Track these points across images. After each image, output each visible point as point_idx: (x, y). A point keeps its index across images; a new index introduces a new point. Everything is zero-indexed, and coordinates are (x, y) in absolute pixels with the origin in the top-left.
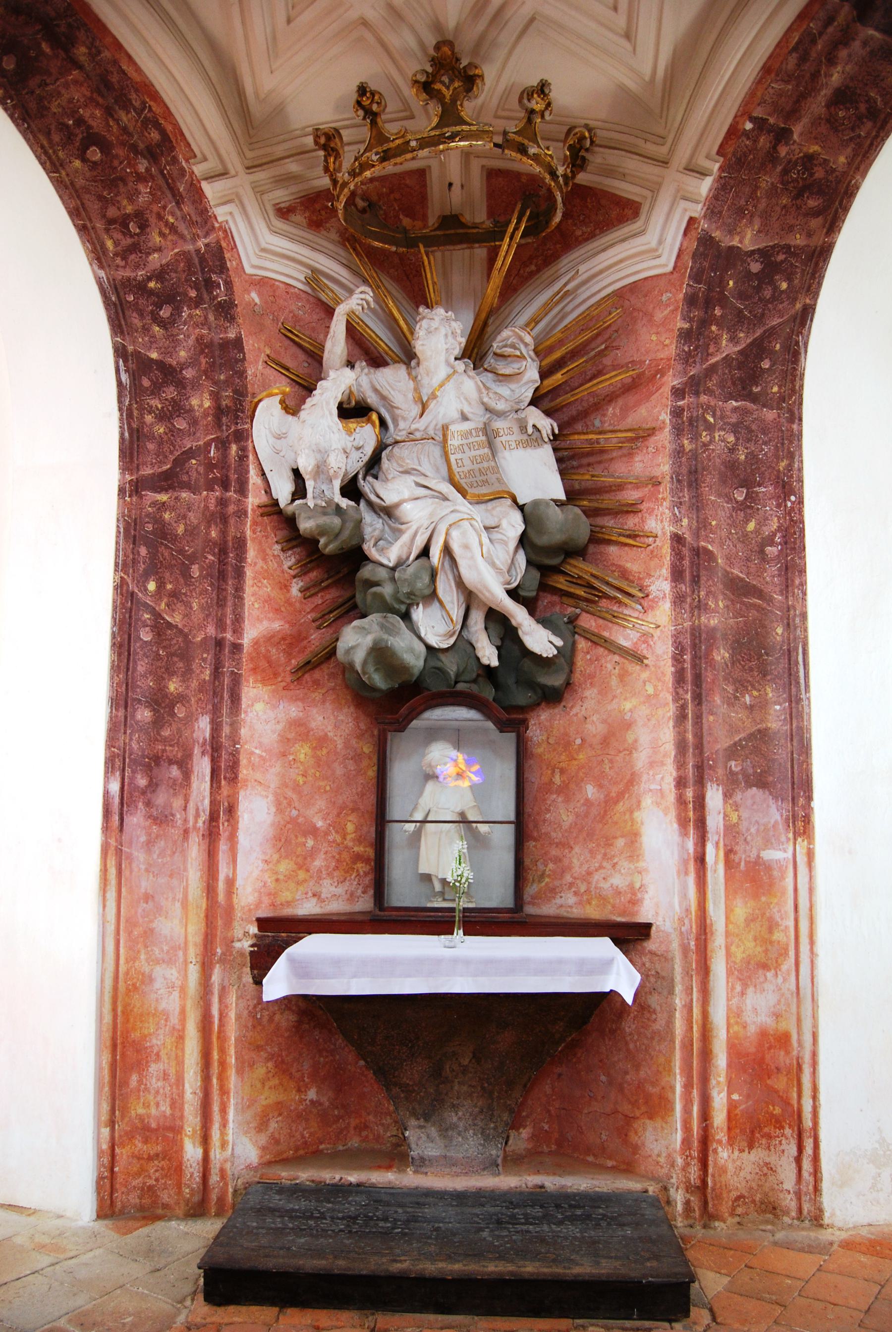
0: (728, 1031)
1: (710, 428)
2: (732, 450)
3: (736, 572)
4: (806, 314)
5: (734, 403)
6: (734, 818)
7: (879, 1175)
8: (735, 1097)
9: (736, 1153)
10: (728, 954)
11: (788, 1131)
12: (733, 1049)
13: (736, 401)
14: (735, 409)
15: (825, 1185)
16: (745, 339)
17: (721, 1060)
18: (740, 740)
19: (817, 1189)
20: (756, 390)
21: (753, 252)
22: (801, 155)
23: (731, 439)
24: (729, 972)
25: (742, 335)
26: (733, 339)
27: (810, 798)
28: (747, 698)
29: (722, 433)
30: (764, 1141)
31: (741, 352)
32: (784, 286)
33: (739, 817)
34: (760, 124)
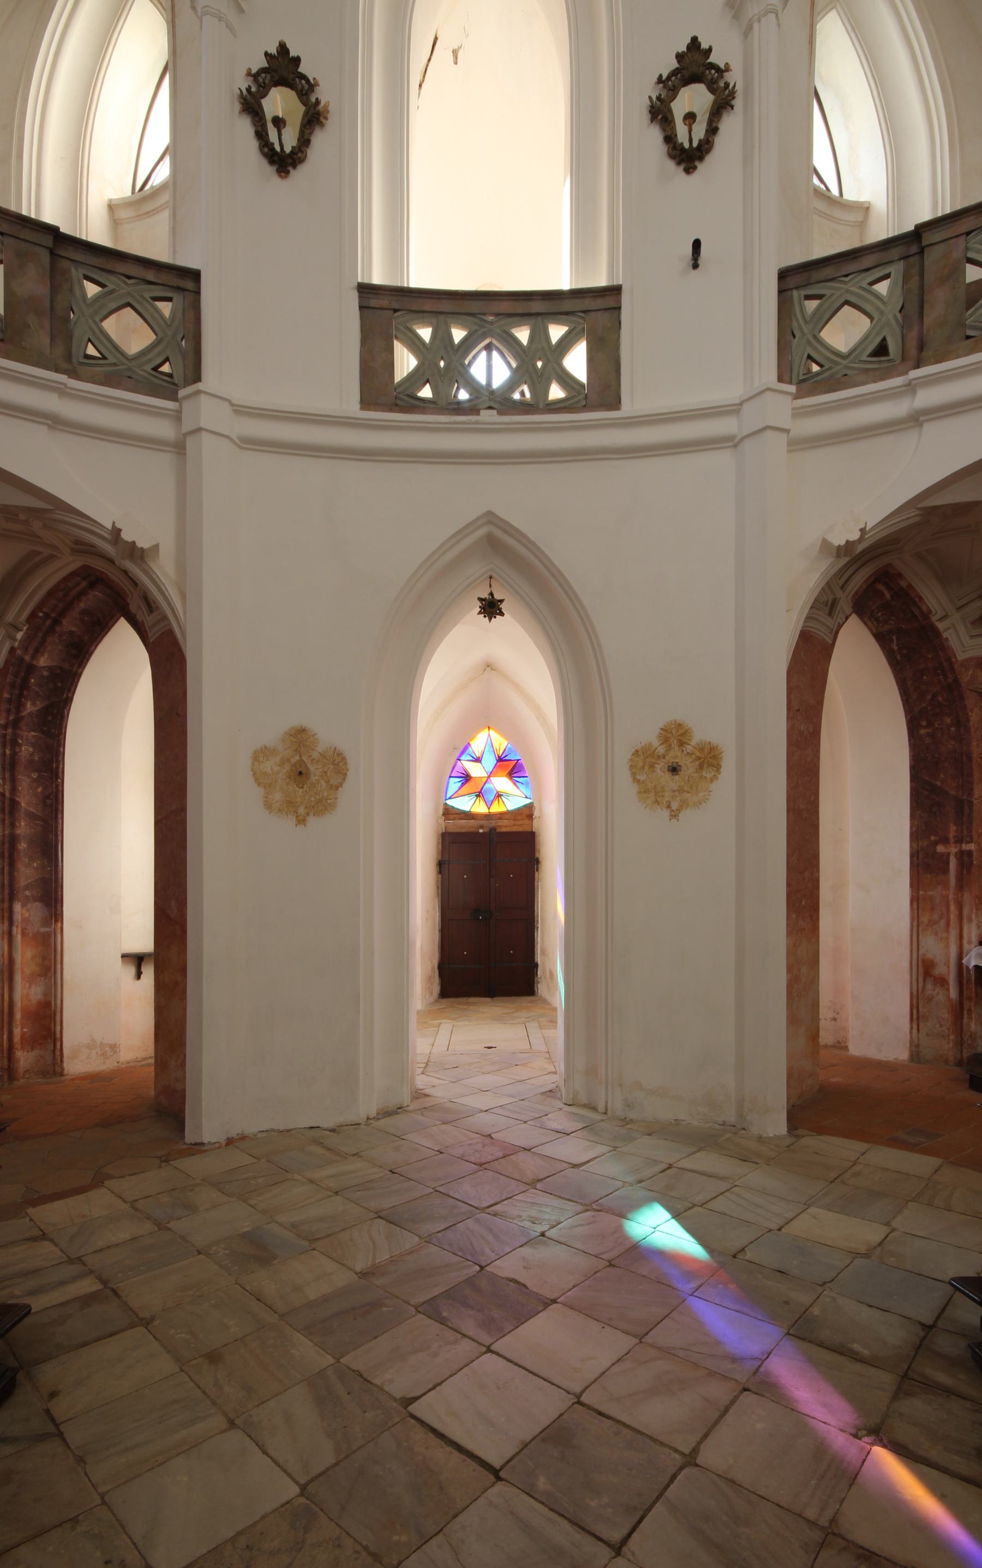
0: (21, 1004)
1: (20, 745)
2: (32, 755)
3: (31, 809)
4: (68, 701)
5: (33, 734)
6: (27, 915)
7: (91, 1053)
8: (25, 1030)
9: (26, 1053)
10: (23, 972)
11: (49, 1040)
12: (23, 1010)
13: (35, 732)
14: (34, 736)
15: (65, 1059)
16: (40, 705)
17: (18, 1015)
18: (31, 882)
19: (62, 1061)
20: (45, 729)
21: (44, 667)
22: (68, 630)
23: (31, 749)
24: (23, 979)
25: (38, 703)
26: (34, 704)
27: (62, 906)
28: (35, 864)
29: (26, 747)
30: (39, 1047)
31: (38, 710)
32: (59, 685)
33: (30, 915)
34: (47, 616)
